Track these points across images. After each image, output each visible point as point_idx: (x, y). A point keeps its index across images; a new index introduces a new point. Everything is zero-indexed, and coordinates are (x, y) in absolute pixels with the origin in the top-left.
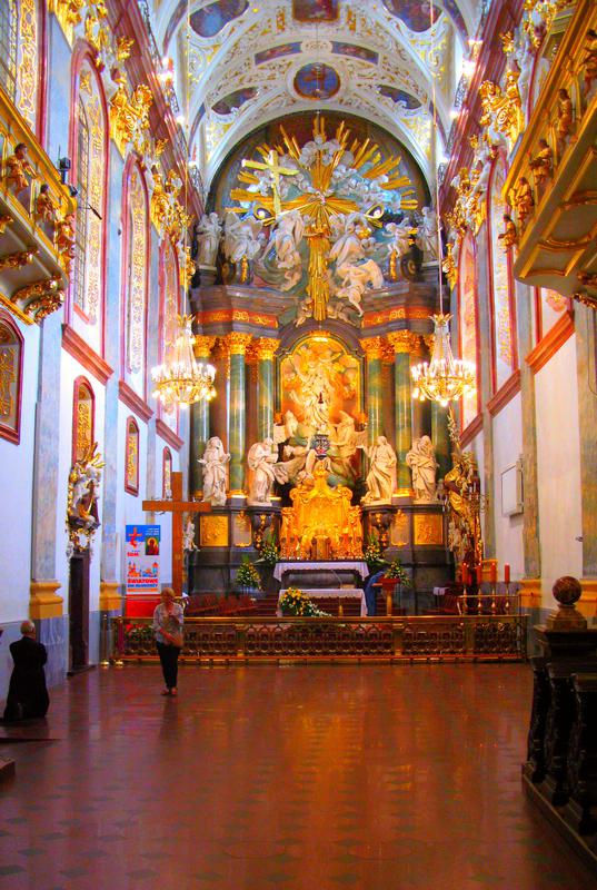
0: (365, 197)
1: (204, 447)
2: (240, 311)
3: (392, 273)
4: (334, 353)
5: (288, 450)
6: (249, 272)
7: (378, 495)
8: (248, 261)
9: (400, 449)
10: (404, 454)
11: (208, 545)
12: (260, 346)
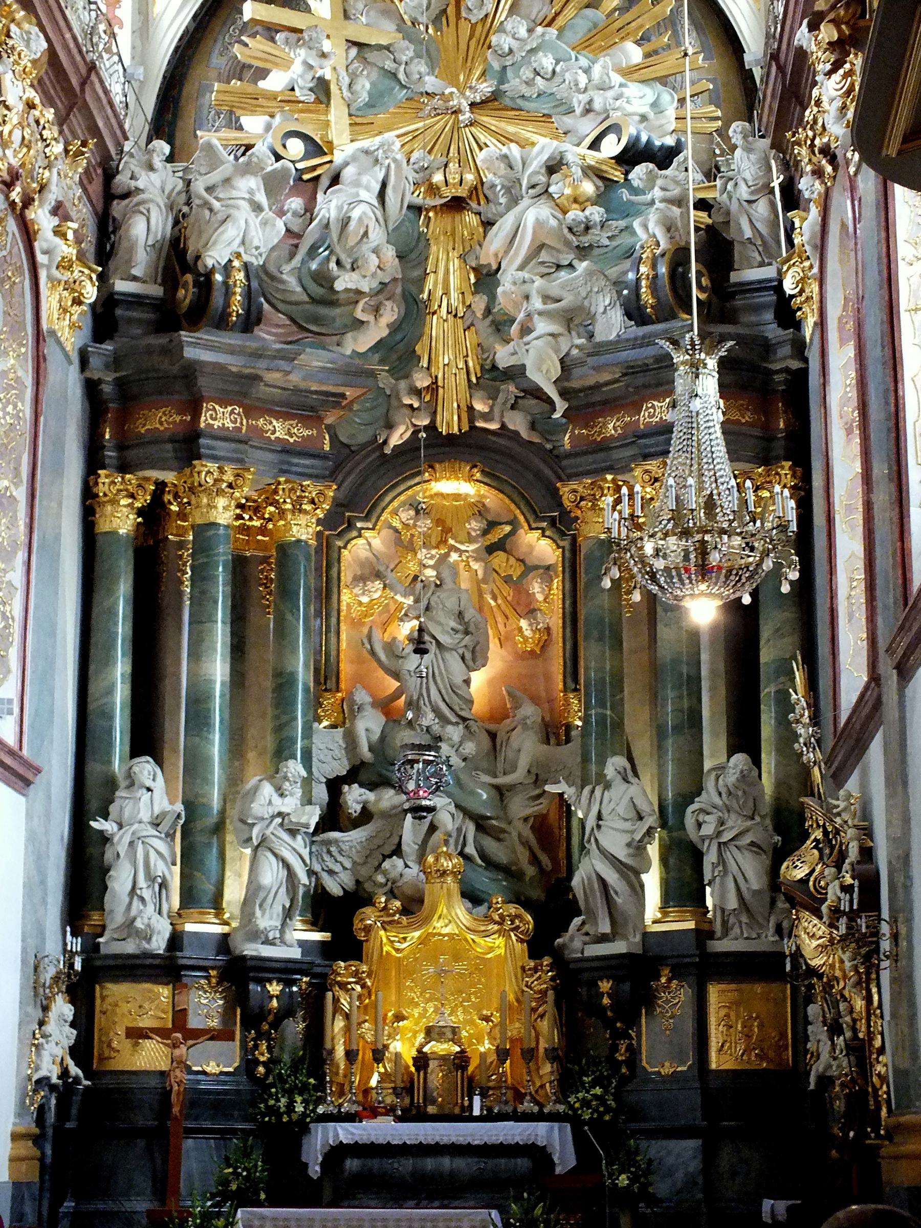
0: (578, 101)
1: (111, 784)
2: (224, 403)
4: (492, 525)
6: (248, 294)
7: (605, 927)
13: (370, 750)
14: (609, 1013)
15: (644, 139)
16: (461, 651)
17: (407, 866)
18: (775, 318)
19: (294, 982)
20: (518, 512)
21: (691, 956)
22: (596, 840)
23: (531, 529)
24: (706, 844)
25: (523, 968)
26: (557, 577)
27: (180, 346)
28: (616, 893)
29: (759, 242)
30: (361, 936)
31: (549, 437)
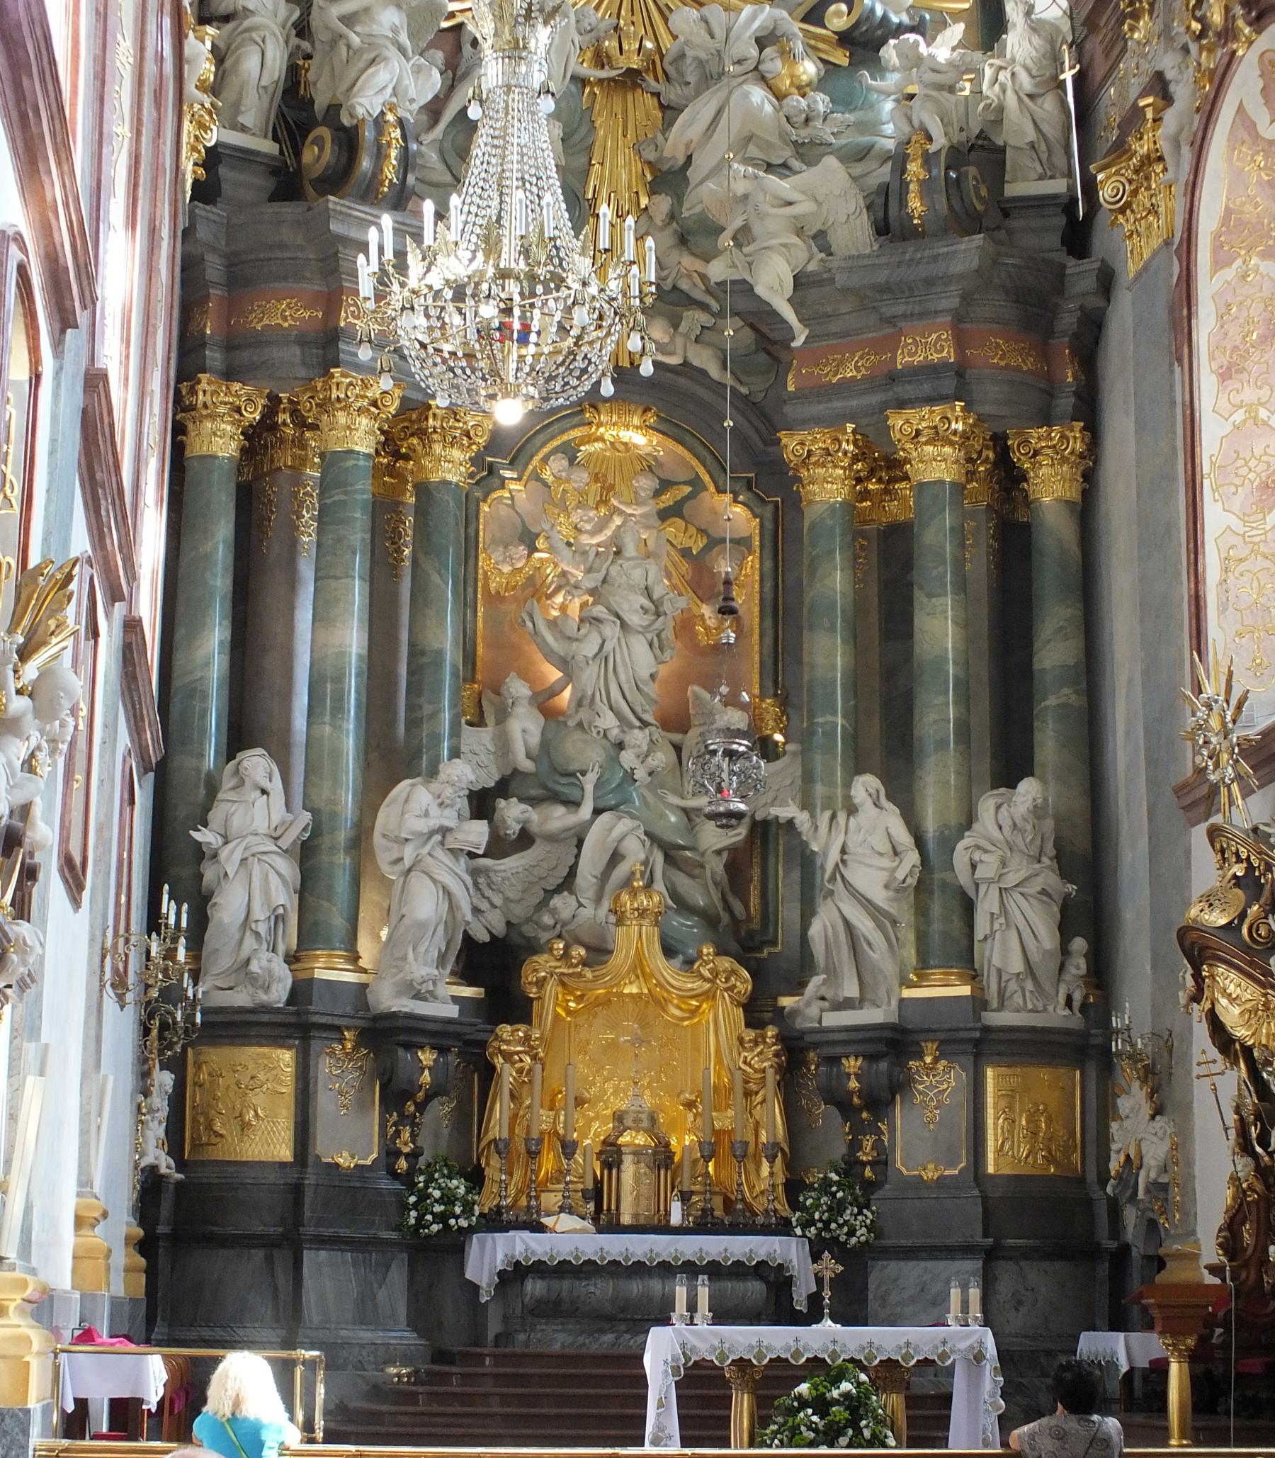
3: (915, 204)
5: (512, 812)
7: (851, 989)
8: (401, 123)
9: (931, 827)
10: (948, 843)
11: (219, 1153)
12: (422, 433)
13: (528, 756)
14: (856, 1100)
15: (879, 11)
16: (649, 636)
17: (580, 905)
18: (1063, 243)
20: (702, 471)
21: (971, 1029)
22: (843, 877)
23: (720, 491)
24: (982, 889)
25: (741, 1041)
26: (750, 552)
27: (326, 216)
28: (869, 944)
29: (1043, 147)
30: (533, 992)
31: (744, 378)
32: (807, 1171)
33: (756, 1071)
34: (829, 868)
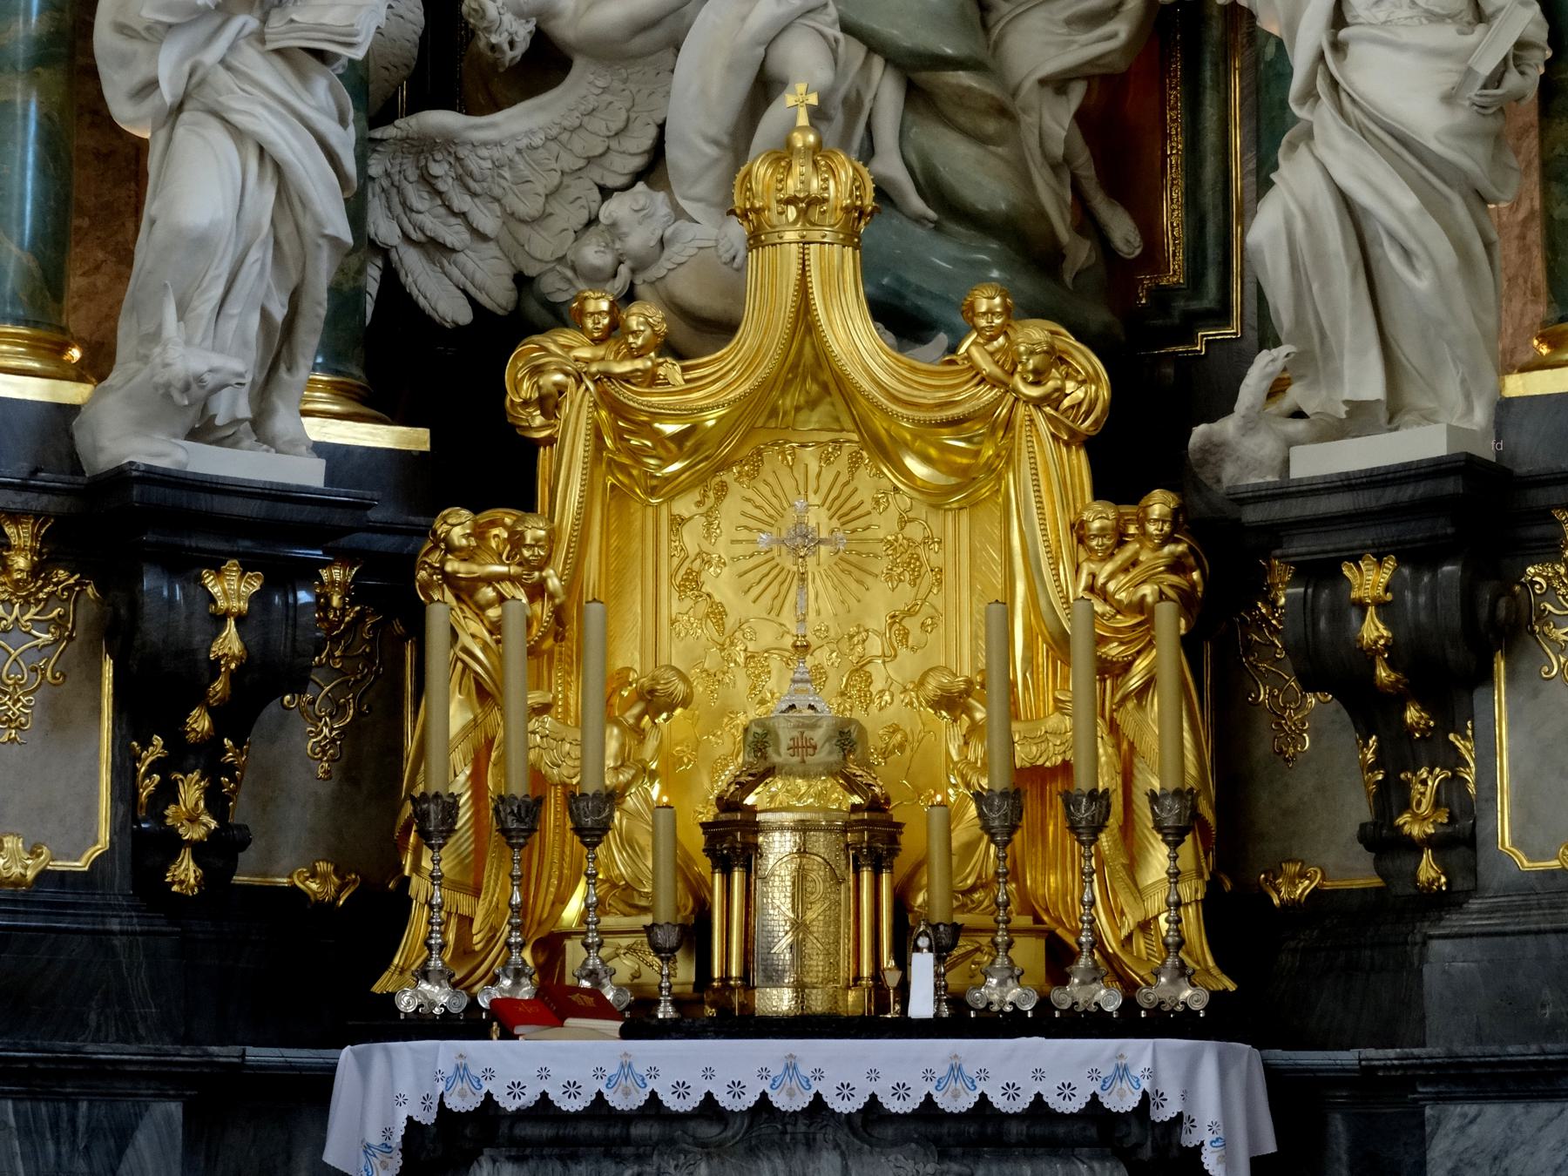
14: (1382, 673)
17: (679, 213)
19: (307, 573)
22: (1334, 84)
25: (1079, 532)
32: (1275, 872)
33: (1120, 609)
34: (1301, 60)
